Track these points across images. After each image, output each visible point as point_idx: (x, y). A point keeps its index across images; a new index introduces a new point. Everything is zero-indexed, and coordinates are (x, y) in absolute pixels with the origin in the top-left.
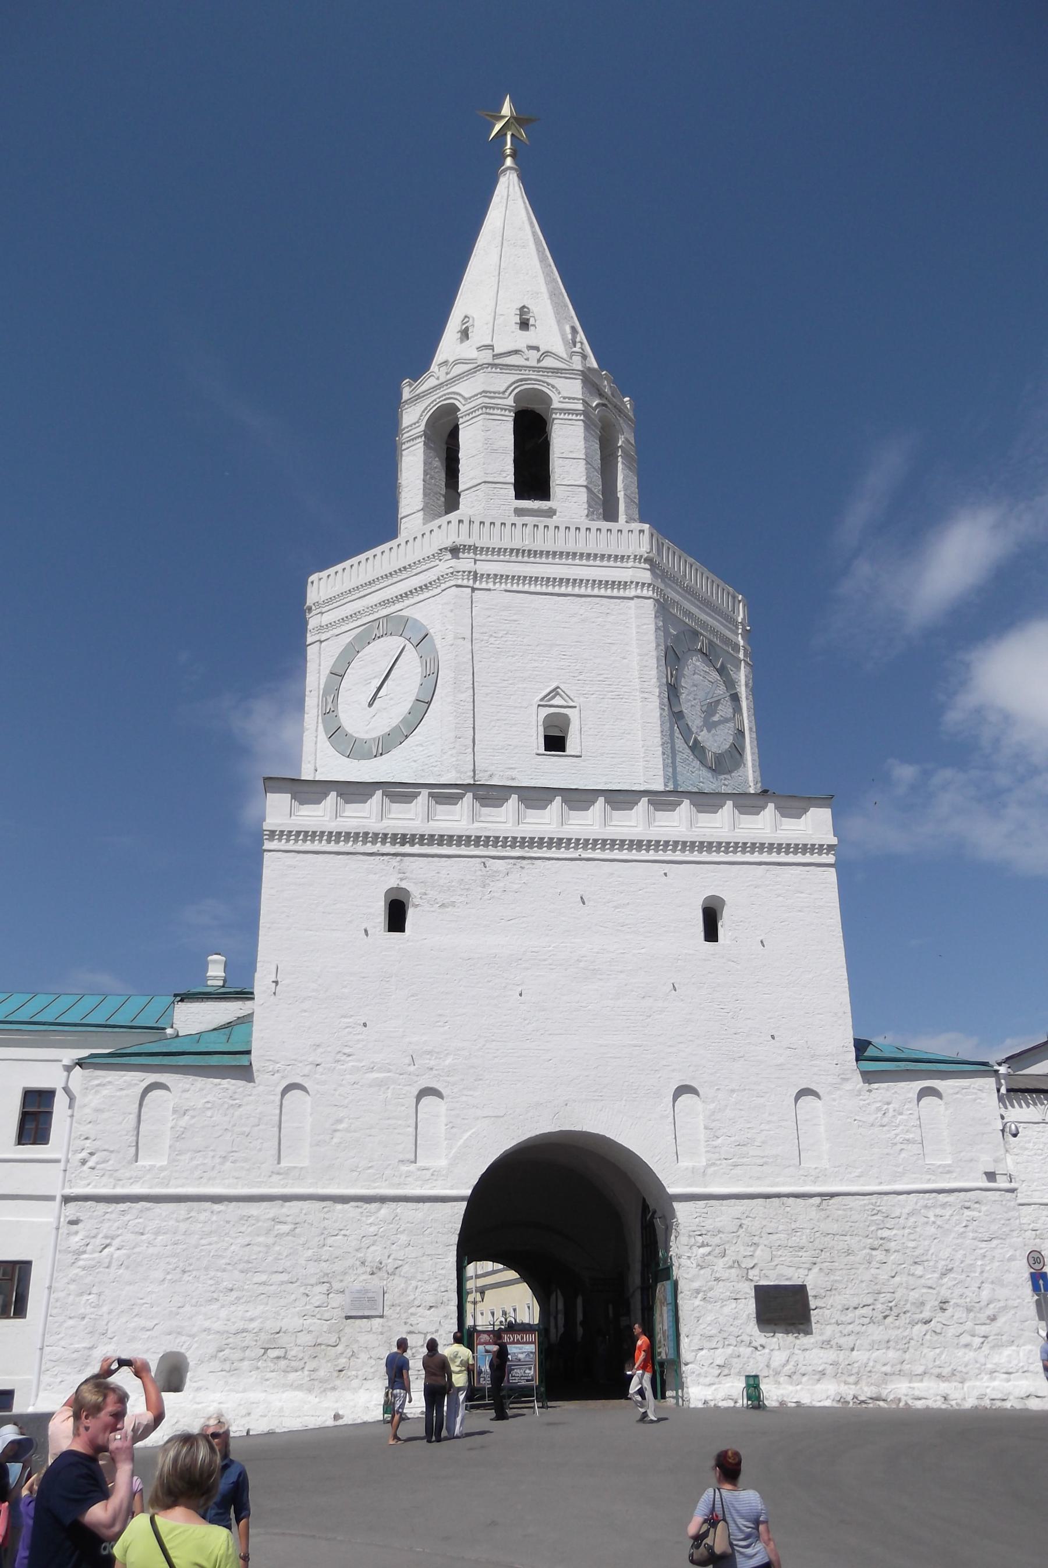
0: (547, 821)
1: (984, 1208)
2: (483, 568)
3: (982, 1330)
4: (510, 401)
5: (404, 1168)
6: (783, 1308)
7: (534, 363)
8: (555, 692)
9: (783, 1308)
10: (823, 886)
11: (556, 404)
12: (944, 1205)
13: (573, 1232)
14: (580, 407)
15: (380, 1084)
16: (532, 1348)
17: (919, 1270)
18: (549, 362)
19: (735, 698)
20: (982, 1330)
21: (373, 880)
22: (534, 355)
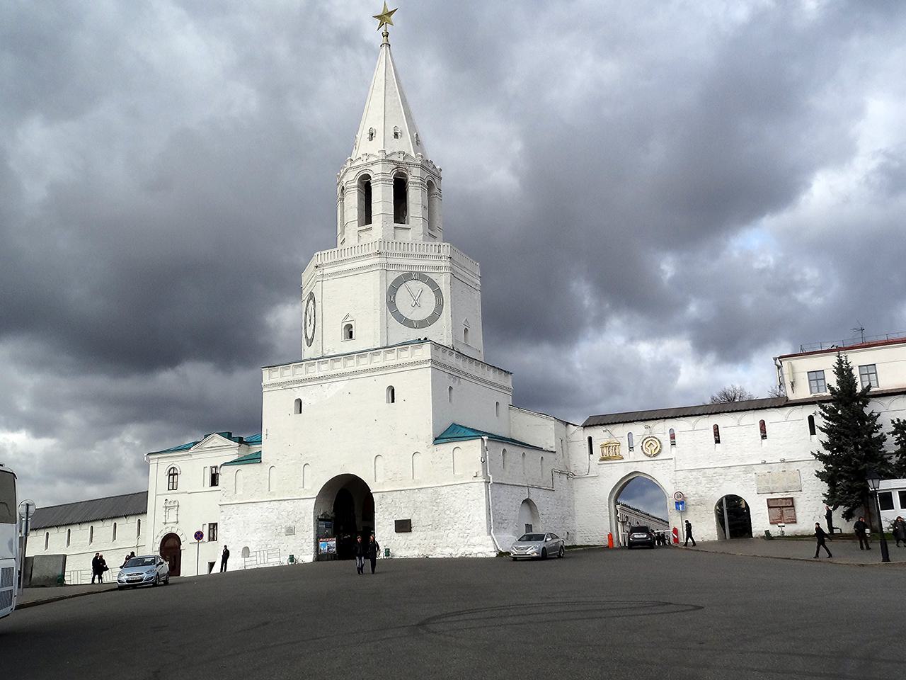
0: (339, 367)
1: (473, 489)
2: (326, 272)
3: (468, 531)
4: (356, 183)
5: (300, 490)
6: (403, 526)
7: (365, 162)
8: (348, 316)
9: (403, 526)
10: (424, 377)
11: (372, 179)
12: (458, 490)
13: (347, 507)
14: (380, 177)
15: (294, 464)
16: (335, 542)
17: (448, 512)
18: (372, 159)
19: (438, 293)
20: (468, 531)
21: (289, 397)
22: (365, 157)
